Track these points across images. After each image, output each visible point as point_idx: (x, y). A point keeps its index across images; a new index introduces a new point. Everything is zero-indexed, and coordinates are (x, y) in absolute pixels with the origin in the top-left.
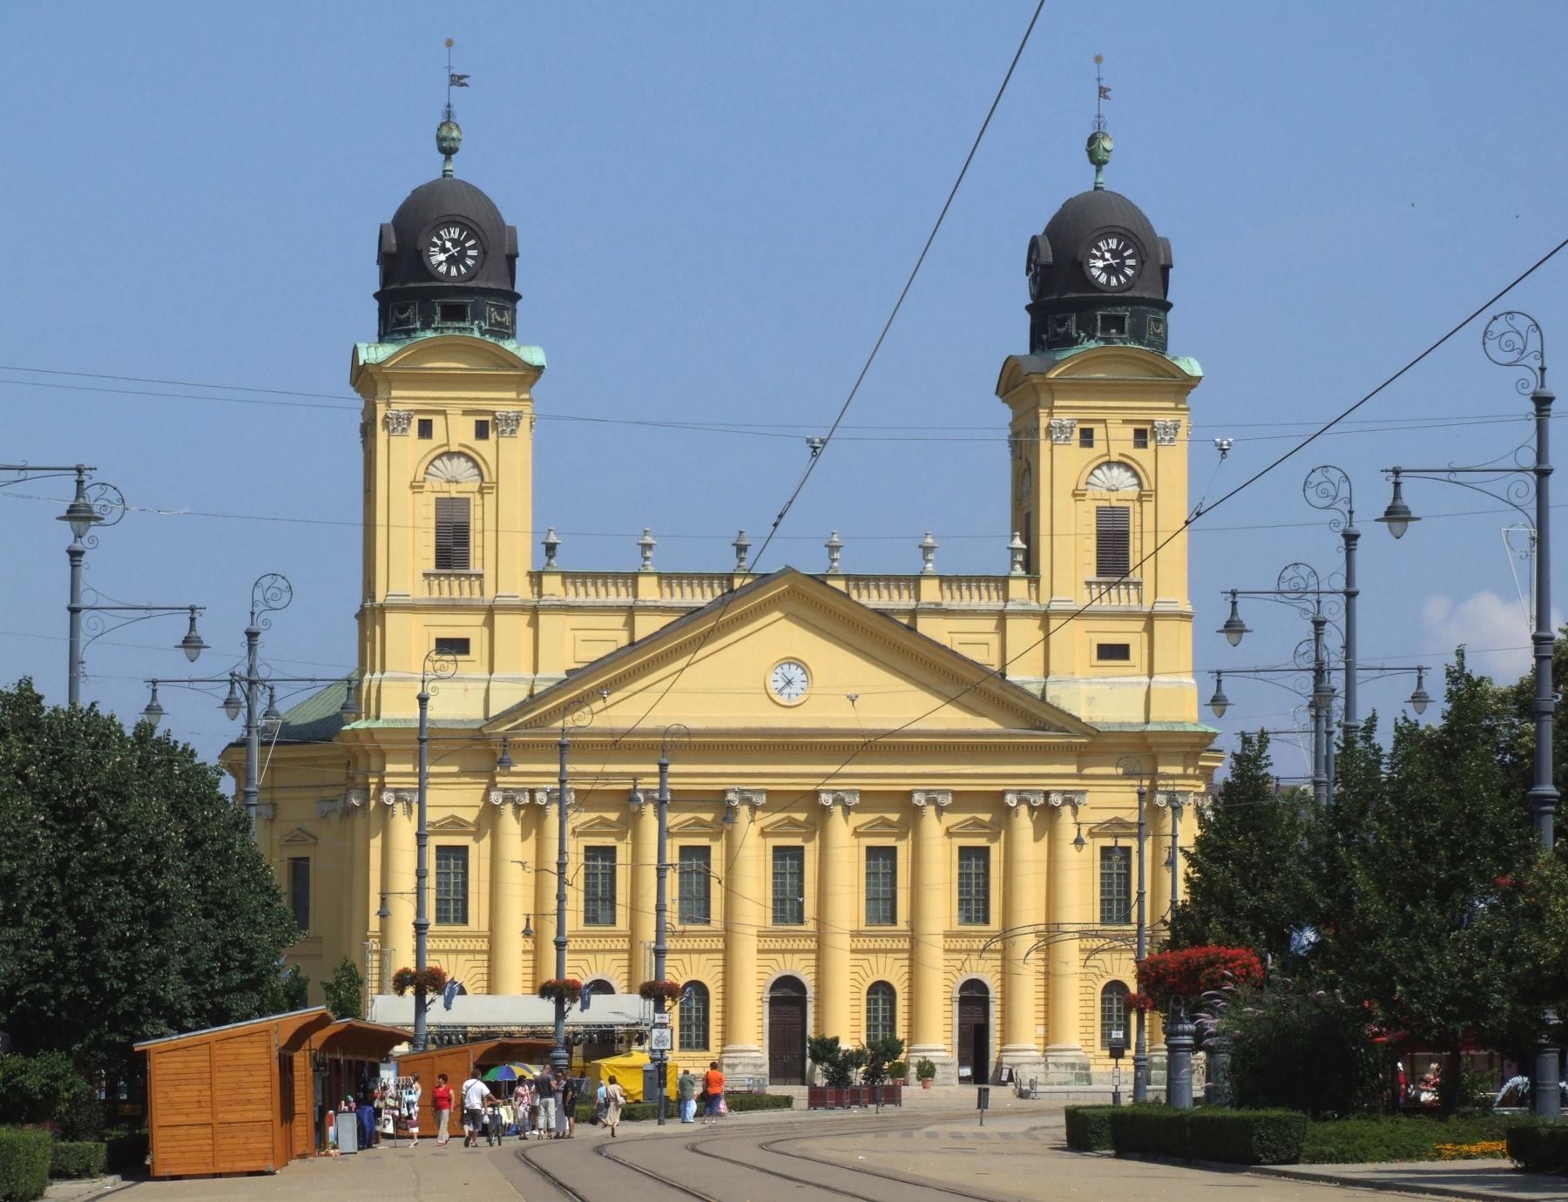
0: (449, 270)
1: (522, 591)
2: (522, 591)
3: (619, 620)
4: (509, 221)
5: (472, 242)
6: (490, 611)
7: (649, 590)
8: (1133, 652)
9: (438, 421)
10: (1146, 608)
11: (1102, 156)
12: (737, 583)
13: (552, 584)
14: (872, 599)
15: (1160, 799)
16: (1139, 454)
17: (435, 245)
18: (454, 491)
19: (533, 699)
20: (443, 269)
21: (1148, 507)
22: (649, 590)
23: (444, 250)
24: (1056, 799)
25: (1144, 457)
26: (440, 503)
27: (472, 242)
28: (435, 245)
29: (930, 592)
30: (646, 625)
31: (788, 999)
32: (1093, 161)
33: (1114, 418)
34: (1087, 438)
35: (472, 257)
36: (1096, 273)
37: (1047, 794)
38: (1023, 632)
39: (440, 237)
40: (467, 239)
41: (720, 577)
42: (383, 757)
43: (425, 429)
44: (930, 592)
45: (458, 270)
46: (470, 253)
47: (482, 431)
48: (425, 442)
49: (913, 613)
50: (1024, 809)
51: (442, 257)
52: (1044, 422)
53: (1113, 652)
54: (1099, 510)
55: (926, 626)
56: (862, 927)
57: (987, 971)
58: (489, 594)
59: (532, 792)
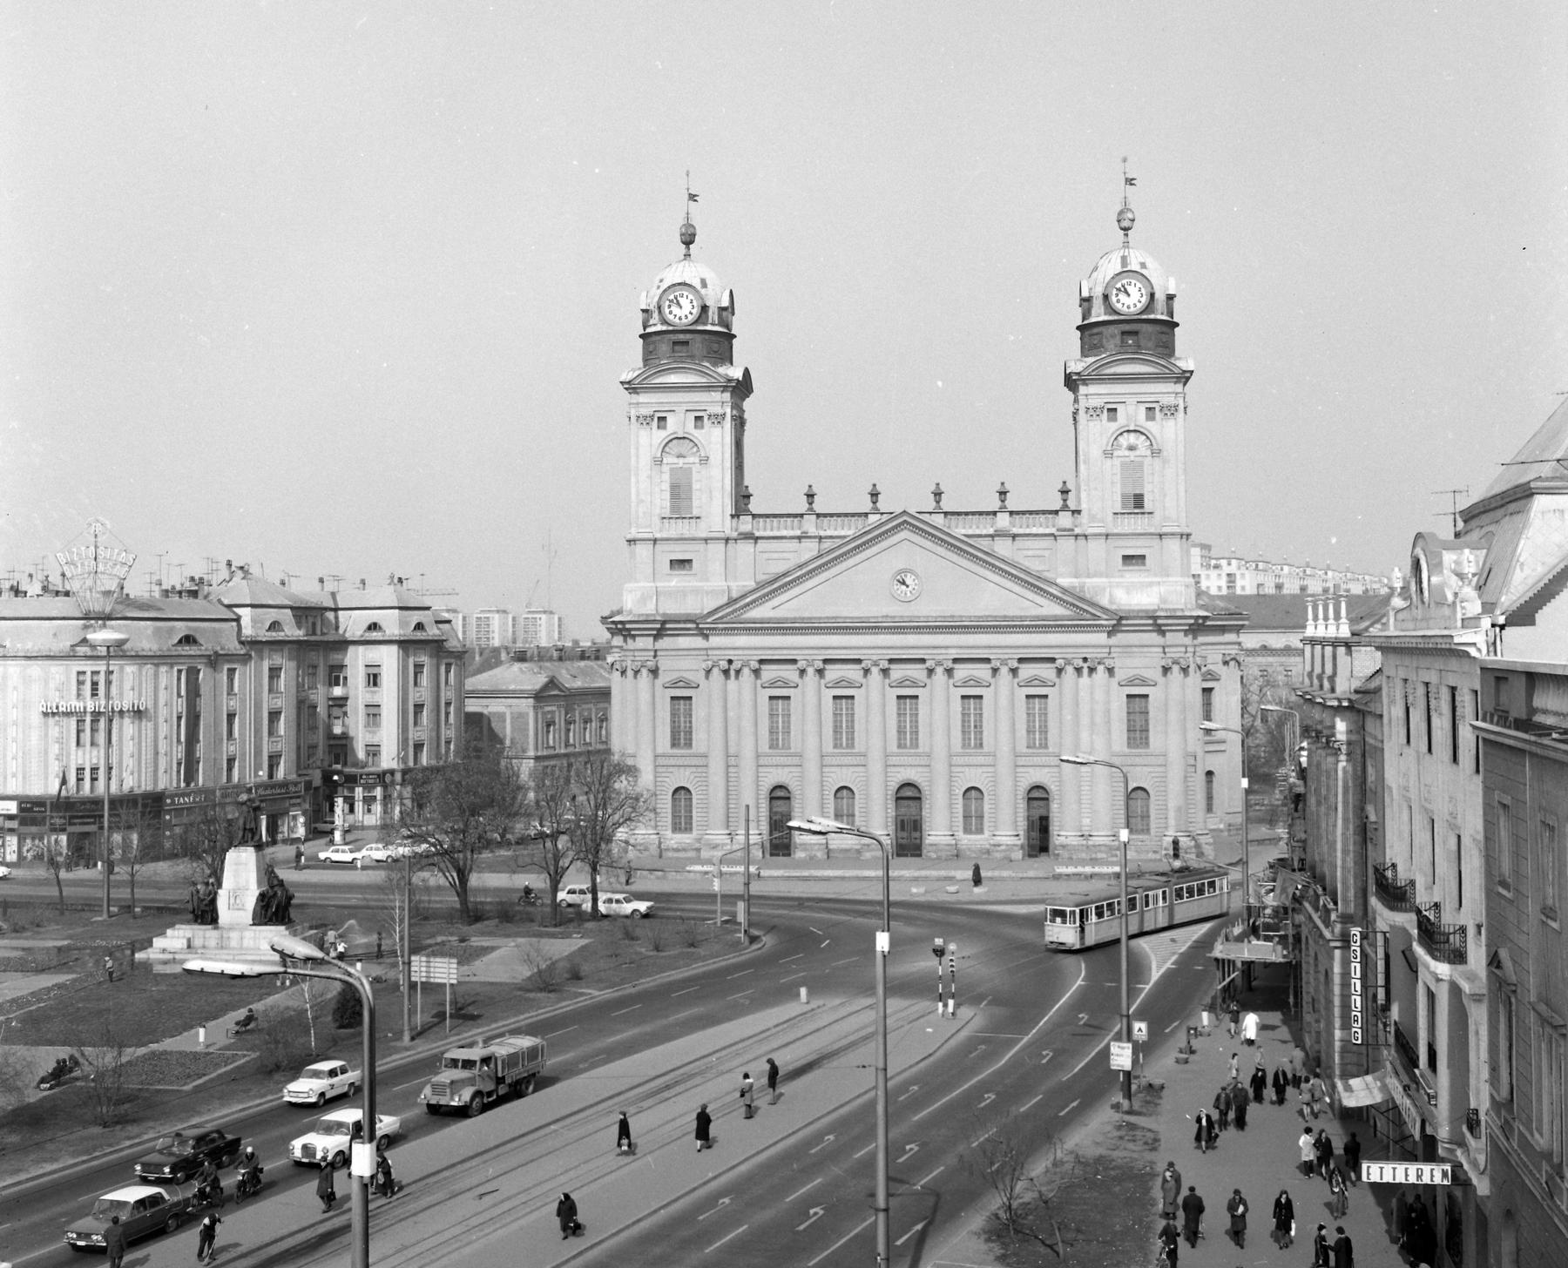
2: (727, 527)
8: (1148, 560)
11: (1126, 224)
14: (960, 529)
16: (1150, 425)
25: (1152, 427)
29: (1003, 521)
30: (809, 549)
33: (1132, 400)
42: (634, 637)
44: (1003, 521)
55: (1003, 548)
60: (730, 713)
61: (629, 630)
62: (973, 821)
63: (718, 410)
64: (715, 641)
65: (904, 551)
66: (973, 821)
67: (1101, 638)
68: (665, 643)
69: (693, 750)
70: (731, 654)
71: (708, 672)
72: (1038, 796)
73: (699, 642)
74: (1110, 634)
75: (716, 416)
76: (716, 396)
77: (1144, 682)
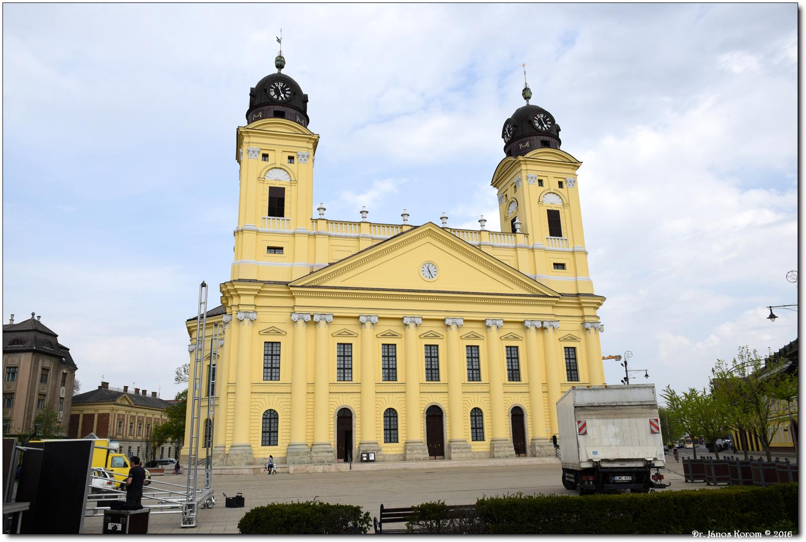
1: (311, 229)
3: (354, 243)
4: (304, 93)
6: (294, 234)
7: (365, 230)
8: (567, 266)
9: (271, 154)
10: (571, 249)
11: (528, 94)
12: (405, 229)
13: (322, 225)
15: (588, 325)
18: (277, 185)
19: (312, 273)
21: (567, 210)
22: (365, 230)
24: (546, 324)
26: (272, 189)
31: (435, 418)
32: (525, 98)
34: (541, 182)
36: (537, 125)
37: (542, 323)
38: (523, 255)
41: (397, 226)
42: (239, 296)
43: (265, 156)
49: (480, 245)
50: (533, 328)
52: (524, 174)
53: (559, 266)
54: (549, 211)
56: (466, 381)
57: (521, 401)
58: (292, 231)
59: (312, 316)
60: (309, 355)
61: (236, 290)
62: (478, 432)
63: (304, 152)
64: (299, 301)
65: (427, 250)
66: (478, 432)
67: (549, 310)
68: (261, 302)
69: (282, 381)
70: (312, 311)
71: (294, 322)
72: (517, 415)
73: (288, 303)
74: (553, 307)
75: (303, 156)
76: (305, 144)
77: (573, 339)
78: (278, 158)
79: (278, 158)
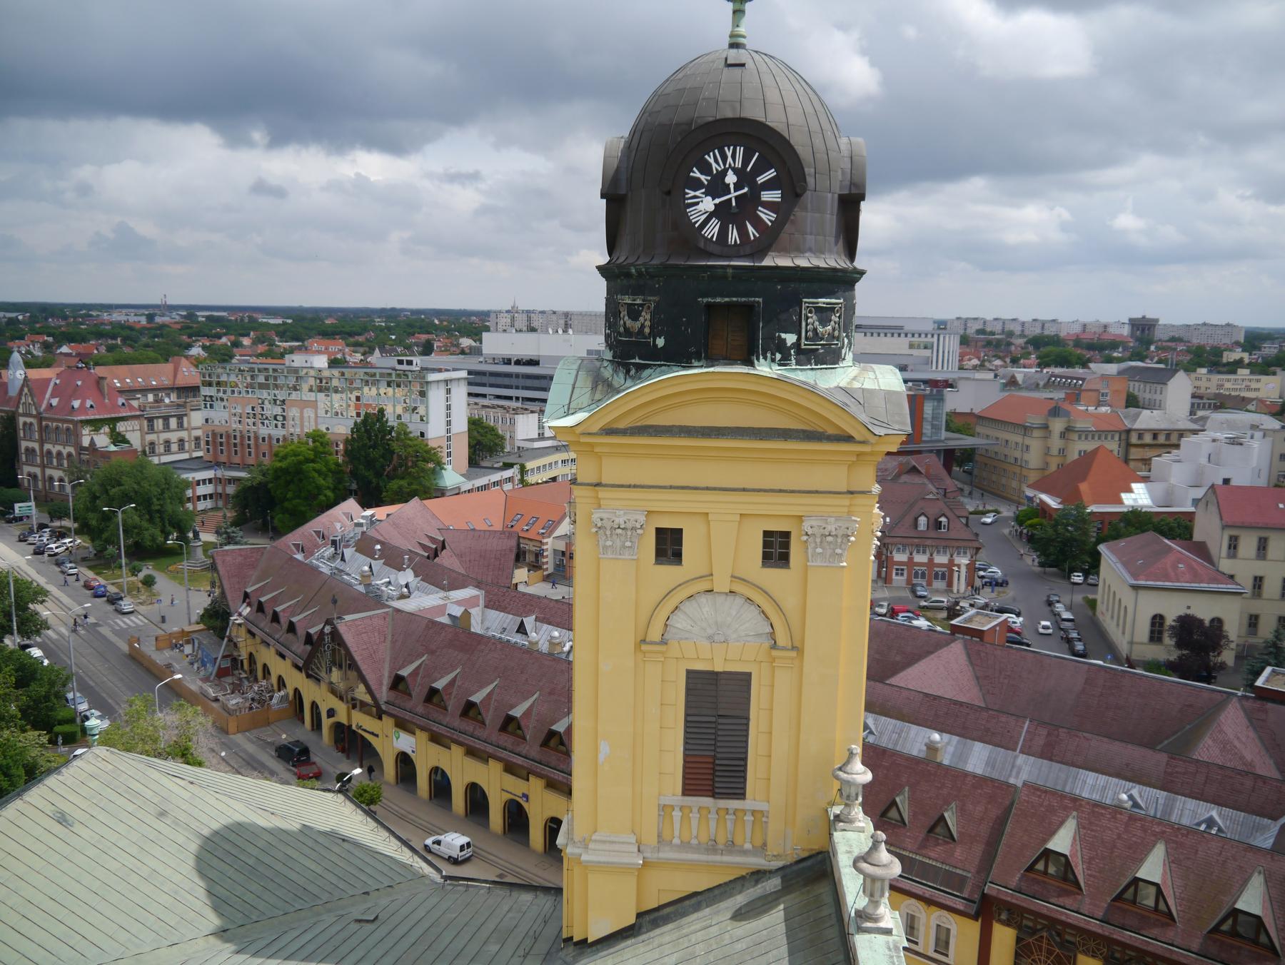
0: (723, 233)
5: (771, 174)
17: (697, 184)
20: (712, 230)
23: (716, 187)
27: (771, 174)
28: (697, 184)
35: (770, 206)
39: (706, 169)
40: (759, 170)
43: (669, 545)
45: (743, 233)
46: (767, 196)
47: (776, 549)
48: (669, 573)
51: (708, 204)
78: (720, 542)
79: (720, 542)
